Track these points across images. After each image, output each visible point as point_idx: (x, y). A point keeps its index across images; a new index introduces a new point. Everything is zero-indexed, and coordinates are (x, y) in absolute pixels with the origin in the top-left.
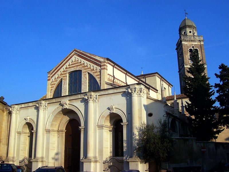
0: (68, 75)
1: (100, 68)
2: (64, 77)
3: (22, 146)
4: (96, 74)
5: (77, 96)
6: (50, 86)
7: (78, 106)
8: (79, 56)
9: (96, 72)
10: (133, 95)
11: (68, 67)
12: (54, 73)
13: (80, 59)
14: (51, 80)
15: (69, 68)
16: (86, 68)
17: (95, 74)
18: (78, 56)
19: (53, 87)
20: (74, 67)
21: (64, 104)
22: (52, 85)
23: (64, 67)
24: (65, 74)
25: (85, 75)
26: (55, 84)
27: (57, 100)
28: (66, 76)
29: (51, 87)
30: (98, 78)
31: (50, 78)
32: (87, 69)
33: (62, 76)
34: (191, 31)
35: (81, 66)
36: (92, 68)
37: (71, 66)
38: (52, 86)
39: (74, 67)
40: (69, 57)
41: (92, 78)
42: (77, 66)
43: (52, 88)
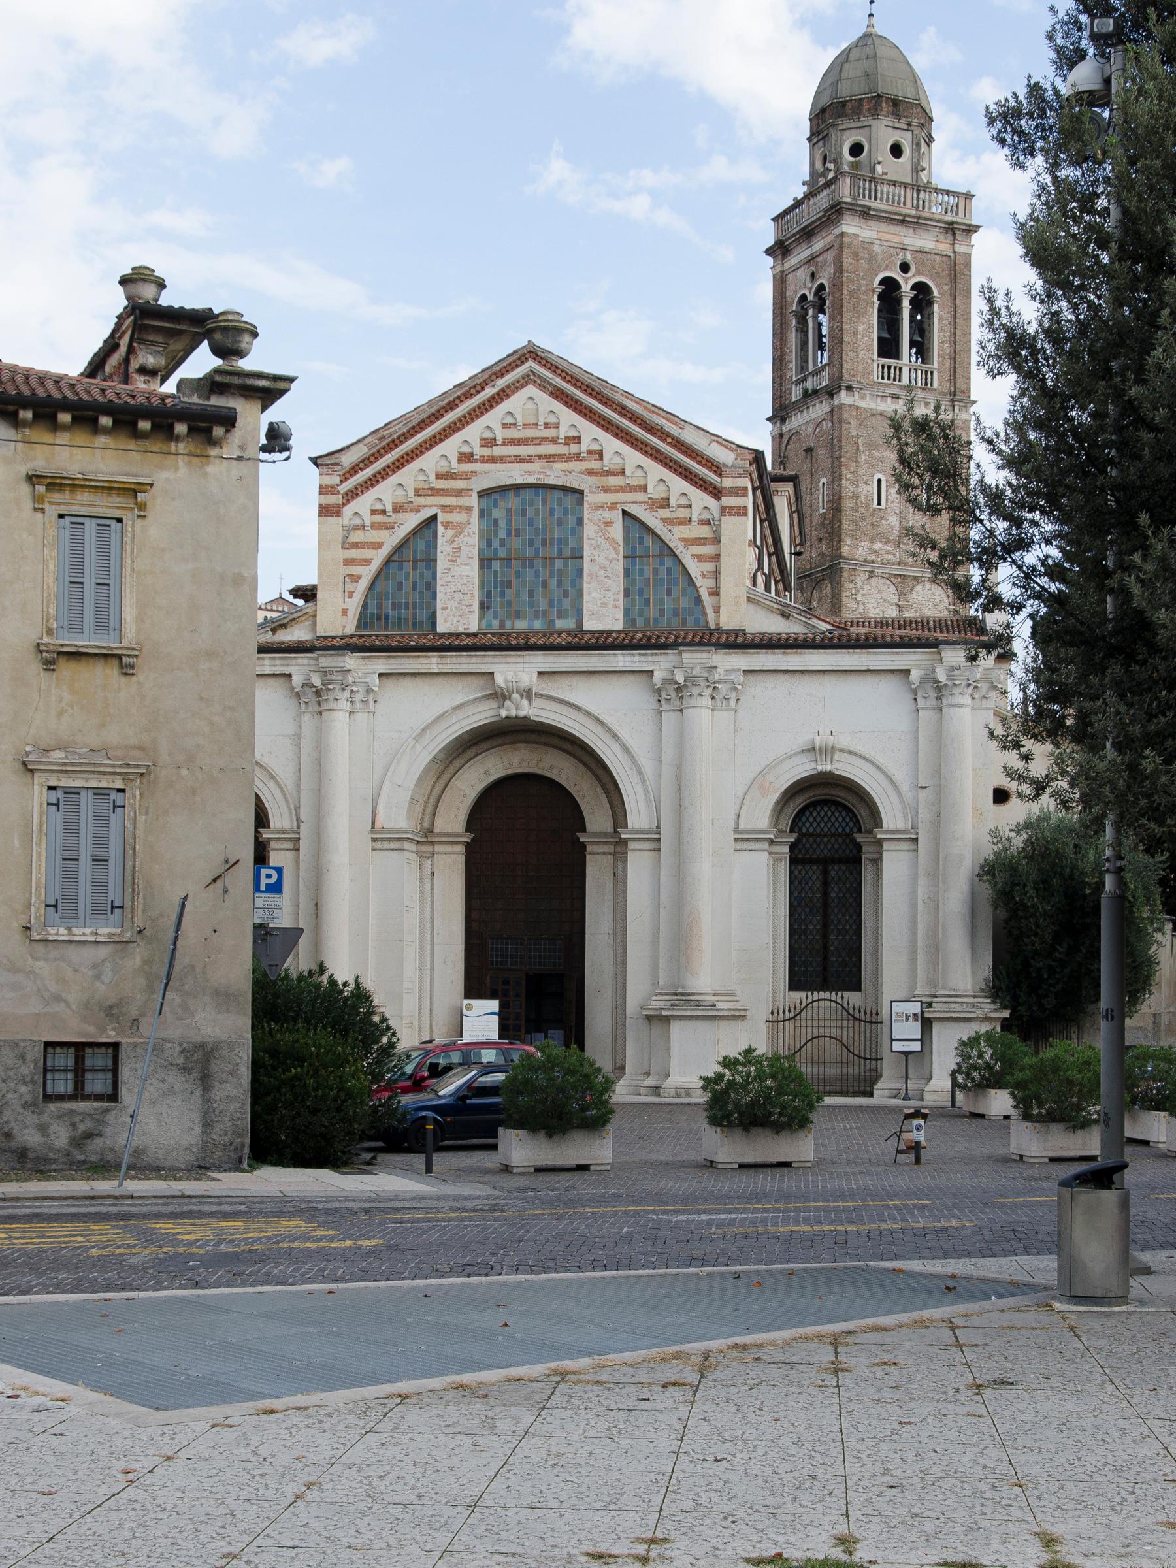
0: (473, 501)
2: (445, 508)
7: (604, 707)
8: (559, 395)
12: (368, 472)
13: (568, 419)
14: (348, 511)
16: (613, 481)
17: (676, 529)
18: (552, 394)
19: (367, 562)
20: (528, 459)
21: (516, 696)
22: (356, 546)
23: (451, 447)
24: (459, 493)
25: (609, 524)
26: (378, 546)
27: (455, 660)
32: (620, 490)
33: (430, 500)
38: (353, 554)
39: (528, 459)
40: (489, 391)
41: (643, 544)
43: (355, 570)
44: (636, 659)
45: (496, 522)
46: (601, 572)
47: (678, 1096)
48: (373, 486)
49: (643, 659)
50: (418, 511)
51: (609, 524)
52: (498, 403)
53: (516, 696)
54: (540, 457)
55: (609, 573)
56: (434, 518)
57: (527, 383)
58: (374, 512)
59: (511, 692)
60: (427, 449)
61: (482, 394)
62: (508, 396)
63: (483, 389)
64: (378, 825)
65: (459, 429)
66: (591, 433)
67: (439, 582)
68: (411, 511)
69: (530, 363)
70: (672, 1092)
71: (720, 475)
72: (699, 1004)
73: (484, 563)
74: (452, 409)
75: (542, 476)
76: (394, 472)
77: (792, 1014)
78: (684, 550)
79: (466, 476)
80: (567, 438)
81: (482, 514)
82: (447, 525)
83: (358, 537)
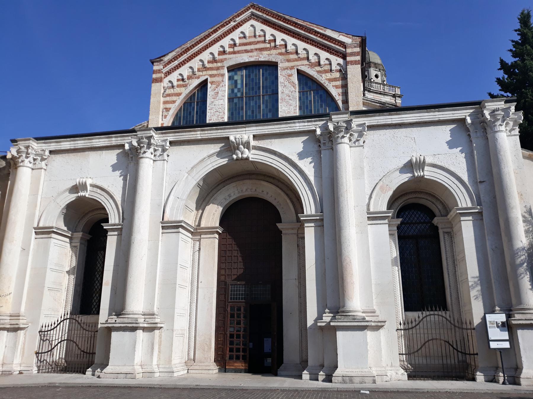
1: (341, 61)
2: (211, 76)
3: (50, 278)
4: (329, 76)
5: (290, 125)
6: (162, 99)
9: (326, 72)
10: (497, 128)
11: (227, 49)
12: (176, 63)
13: (270, 31)
14: (166, 80)
15: (230, 53)
17: (323, 75)
18: (262, 23)
19: (174, 102)
20: (251, 51)
21: (241, 146)
22: (169, 95)
23: (215, 49)
24: (218, 69)
25: (291, 75)
26: (179, 94)
28: (223, 75)
29: (165, 103)
30: (337, 87)
31: (163, 76)
32: (296, 60)
33: (204, 73)
34: (379, 74)
35: (274, 52)
36: (313, 59)
37: (236, 49)
38: (168, 99)
39: (251, 51)
40: (233, 24)
42: (261, 50)
43: (168, 106)
44: (306, 124)
45: (236, 81)
46: (287, 97)
47: (344, 382)
48: (178, 68)
49: (309, 124)
50: (198, 78)
51: (291, 75)
52: (236, 29)
53: (241, 146)
54: (256, 49)
55: (291, 98)
56: (207, 80)
57: (250, 19)
58: (178, 80)
59: (238, 144)
60: (203, 51)
61: (229, 25)
62: (241, 25)
63: (230, 23)
64: (166, 219)
65: (218, 41)
66: (280, 36)
67: (208, 108)
68: (196, 78)
69: (252, 10)
70: (340, 379)
71: (345, 48)
72: (354, 319)
73: (230, 100)
74: (215, 32)
75: (257, 57)
76: (188, 62)
77: (414, 325)
78: (329, 84)
79: (222, 61)
80: (269, 40)
81: (230, 78)
82: (212, 83)
83: (171, 91)
